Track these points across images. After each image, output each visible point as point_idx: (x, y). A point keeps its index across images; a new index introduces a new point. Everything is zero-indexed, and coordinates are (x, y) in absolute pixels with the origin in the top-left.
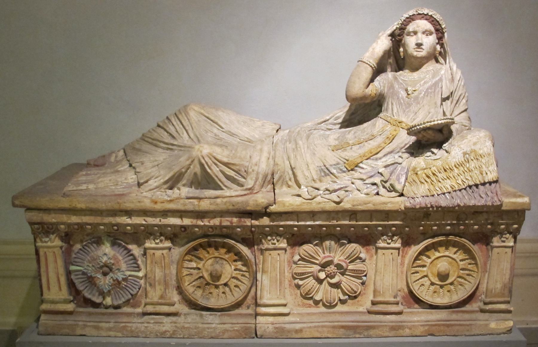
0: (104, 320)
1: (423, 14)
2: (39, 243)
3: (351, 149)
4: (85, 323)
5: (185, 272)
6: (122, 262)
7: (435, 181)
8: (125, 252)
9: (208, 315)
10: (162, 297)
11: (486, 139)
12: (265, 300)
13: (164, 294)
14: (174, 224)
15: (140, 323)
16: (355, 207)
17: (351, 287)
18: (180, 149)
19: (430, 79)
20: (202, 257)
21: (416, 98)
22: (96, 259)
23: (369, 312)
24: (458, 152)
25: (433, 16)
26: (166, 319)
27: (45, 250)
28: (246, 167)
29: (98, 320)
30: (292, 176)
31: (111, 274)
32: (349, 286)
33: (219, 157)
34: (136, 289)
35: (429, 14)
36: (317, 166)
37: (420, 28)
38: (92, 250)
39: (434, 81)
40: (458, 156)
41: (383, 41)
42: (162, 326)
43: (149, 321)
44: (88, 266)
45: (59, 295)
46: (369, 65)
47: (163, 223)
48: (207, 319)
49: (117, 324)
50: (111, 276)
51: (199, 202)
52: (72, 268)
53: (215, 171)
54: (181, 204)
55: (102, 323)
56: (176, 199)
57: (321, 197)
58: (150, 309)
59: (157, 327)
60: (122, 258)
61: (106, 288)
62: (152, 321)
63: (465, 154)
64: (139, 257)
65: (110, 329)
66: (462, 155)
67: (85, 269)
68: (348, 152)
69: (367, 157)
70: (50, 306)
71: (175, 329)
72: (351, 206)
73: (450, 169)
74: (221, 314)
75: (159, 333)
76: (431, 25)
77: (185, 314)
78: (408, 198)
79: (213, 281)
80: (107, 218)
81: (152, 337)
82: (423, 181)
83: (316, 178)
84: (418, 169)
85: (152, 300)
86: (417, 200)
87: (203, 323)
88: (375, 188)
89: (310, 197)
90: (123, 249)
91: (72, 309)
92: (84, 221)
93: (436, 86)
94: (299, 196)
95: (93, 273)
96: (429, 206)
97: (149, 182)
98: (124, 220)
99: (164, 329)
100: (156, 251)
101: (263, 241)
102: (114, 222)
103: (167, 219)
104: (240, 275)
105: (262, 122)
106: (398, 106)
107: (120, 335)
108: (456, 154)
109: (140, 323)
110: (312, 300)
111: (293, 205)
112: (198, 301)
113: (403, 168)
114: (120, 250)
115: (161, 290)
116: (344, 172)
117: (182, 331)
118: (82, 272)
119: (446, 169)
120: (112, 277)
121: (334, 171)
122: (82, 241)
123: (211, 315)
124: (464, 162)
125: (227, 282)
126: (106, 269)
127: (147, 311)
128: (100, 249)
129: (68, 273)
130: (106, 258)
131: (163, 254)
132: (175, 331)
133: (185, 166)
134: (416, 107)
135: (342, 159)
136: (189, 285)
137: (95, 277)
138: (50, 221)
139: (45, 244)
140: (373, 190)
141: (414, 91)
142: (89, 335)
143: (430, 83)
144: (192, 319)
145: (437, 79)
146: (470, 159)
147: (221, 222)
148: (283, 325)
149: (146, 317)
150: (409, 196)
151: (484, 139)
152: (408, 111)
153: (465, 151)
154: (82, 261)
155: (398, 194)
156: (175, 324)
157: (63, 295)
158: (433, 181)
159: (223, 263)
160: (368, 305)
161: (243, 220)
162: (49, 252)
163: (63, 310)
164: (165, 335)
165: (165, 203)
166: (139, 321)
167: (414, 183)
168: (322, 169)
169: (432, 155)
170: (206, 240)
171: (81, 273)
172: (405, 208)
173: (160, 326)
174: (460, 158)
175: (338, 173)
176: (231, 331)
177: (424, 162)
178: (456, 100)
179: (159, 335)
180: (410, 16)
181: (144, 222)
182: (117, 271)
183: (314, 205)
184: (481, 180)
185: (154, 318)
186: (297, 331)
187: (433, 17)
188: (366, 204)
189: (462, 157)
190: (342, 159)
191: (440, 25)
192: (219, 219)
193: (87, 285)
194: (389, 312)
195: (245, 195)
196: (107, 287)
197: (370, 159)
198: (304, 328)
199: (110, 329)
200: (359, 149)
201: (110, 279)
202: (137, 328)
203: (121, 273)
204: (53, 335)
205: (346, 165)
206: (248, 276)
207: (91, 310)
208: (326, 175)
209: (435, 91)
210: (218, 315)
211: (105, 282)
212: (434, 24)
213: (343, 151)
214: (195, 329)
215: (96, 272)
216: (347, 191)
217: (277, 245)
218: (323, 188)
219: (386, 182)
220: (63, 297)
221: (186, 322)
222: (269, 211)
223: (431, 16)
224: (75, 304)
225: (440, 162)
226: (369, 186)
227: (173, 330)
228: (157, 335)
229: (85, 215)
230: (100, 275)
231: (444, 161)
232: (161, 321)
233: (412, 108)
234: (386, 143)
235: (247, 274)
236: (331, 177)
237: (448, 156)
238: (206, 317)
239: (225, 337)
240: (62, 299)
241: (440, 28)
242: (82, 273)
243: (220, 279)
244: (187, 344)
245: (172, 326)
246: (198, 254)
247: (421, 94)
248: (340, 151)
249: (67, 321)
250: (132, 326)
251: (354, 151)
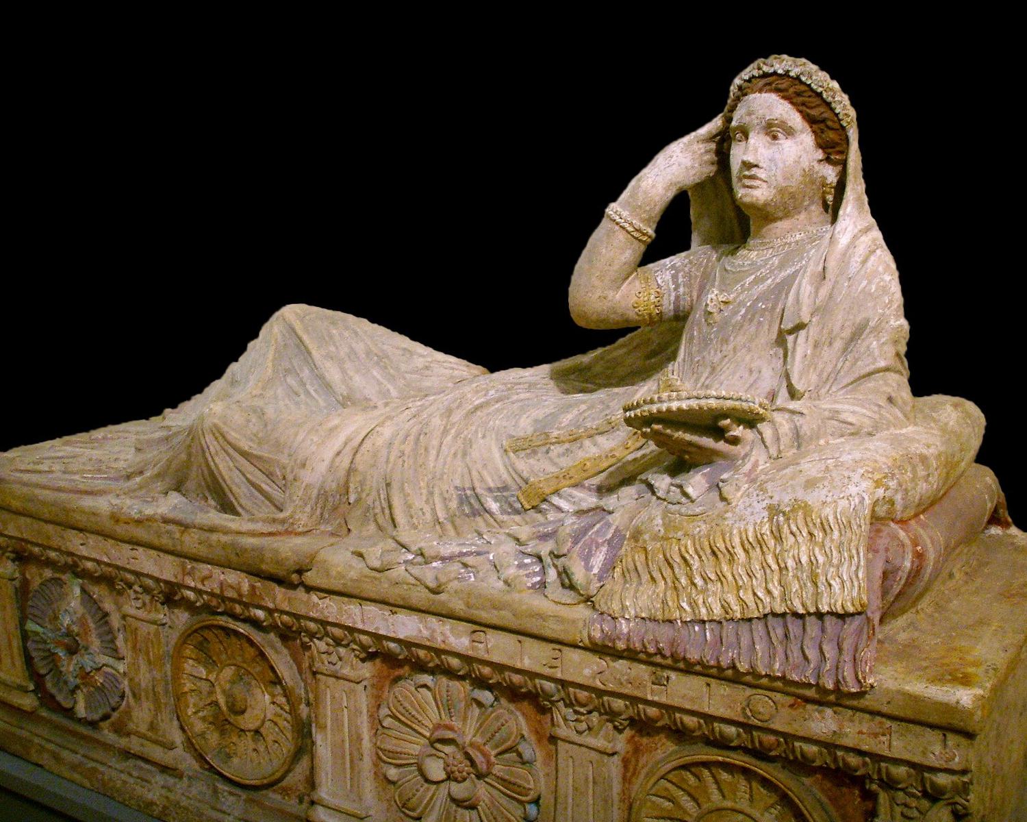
0: (70, 746)
1: (775, 73)
3: (547, 452)
4: (43, 743)
7: (684, 581)
10: (152, 727)
11: (851, 474)
13: (155, 721)
19: (771, 271)
21: (726, 322)
24: (755, 503)
25: (803, 79)
26: (160, 779)
28: (284, 468)
30: (385, 505)
33: (233, 435)
35: (792, 74)
36: (456, 487)
37: (753, 117)
39: (784, 274)
40: (752, 514)
41: (671, 157)
46: (617, 224)
49: (85, 760)
51: (183, 532)
53: (221, 466)
56: (147, 520)
57: (406, 570)
59: (139, 790)
62: (135, 774)
63: (774, 511)
64: (119, 630)
65: (74, 767)
66: (766, 514)
67: (44, 633)
68: (538, 460)
69: (572, 481)
71: (165, 803)
72: (463, 607)
73: (727, 548)
75: (143, 802)
76: (790, 106)
77: (190, 778)
78: (602, 614)
82: (656, 575)
83: (445, 519)
84: (646, 537)
86: (624, 627)
87: (213, 808)
88: (538, 569)
89: (377, 564)
91: (28, 708)
93: (780, 293)
94: (361, 555)
96: (652, 650)
99: (150, 796)
105: (430, 360)
107: (88, 785)
108: (749, 509)
111: (344, 577)
113: (608, 525)
115: (150, 710)
116: (517, 512)
119: (715, 549)
121: (494, 506)
123: (231, 793)
124: (765, 537)
125: (260, 728)
127: (130, 749)
129: (25, 636)
134: (718, 352)
136: (195, 713)
137: (54, 654)
140: (527, 576)
141: (725, 303)
143: (769, 281)
144: (200, 792)
145: (789, 271)
146: (785, 529)
149: (131, 762)
150: (605, 609)
151: (846, 474)
152: (698, 362)
153: (775, 501)
155: (582, 598)
156: (169, 794)
158: (677, 579)
159: (249, 684)
167: (633, 574)
168: (465, 494)
169: (684, 500)
174: (759, 522)
175: (503, 512)
177: (662, 519)
178: (842, 338)
180: (745, 81)
183: (386, 586)
184: (809, 603)
187: (804, 84)
188: (495, 608)
189: (766, 520)
191: (828, 104)
195: (270, 534)
197: (583, 486)
200: (563, 454)
203: (90, 657)
205: (519, 493)
207: (57, 718)
208: (475, 513)
209: (773, 308)
211: (69, 666)
212: (803, 104)
213: (528, 456)
216: (465, 566)
217: (338, 667)
218: (414, 548)
219: (558, 557)
221: (186, 794)
223: (798, 78)
224: (39, 698)
225: (703, 527)
226: (527, 561)
230: (64, 653)
231: (713, 524)
232: (149, 777)
233: (710, 353)
234: (627, 448)
236: (485, 521)
237: (726, 512)
238: (224, 797)
241: (828, 114)
245: (161, 795)
247: (736, 313)
248: (522, 454)
249: (22, 728)
251: (551, 459)
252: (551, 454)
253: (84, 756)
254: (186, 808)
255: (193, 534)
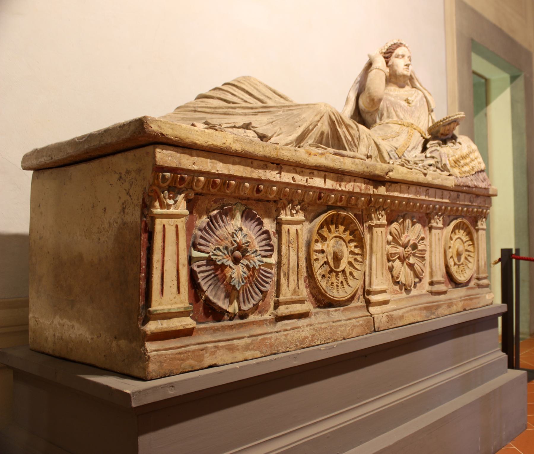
2: (158, 209)
5: (314, 256)
6: (256, 242)
8: (258, 227)
9: (333, 312)
10: (295, 292)
12: (375, 287)
14: (318, 186)
15: (277, 332)
16: (434, 180)
17: (421, 268)
18: (289, 108)
20: (326, 236)
22: (227, 238)
23: (432, 293)
27: (165, 221)
29: (229, 337)
31: (244, 261)
32: (420, 267)
34: (267, 283)
38: (219, 226)
42: (301, 330)
43: (284, 328)
44: (218, 249)
45: (176, 303)
47: (309, 185)
48: (333, 316)
50: (245, 264)
52: (195, 254)
54: (331, 159)
55: (235, 341)
58: (283, 310)
60: (255, 238)
61: (239, 282)
65: (247, 348)
70: (162, 324)
71: (314, 333)
74: (344, 308)
79: (335, 268)
80: (257, 171)
81: (292, 349)
85: (286, 298)
90: (256, 223)
92: (231, 173)
95: (226, 260)
97: (272, 139)
98: (272, 175)
99: (303, 334)
100: (291, 226)
101: (373, 215)
102: (263, 178)
103: (313, 179)
104: (354, 258)
106: (403, 113)
109: (277, 332)
110: (398, 286)
112: (327, 293)
114: (251, 226)
117: (320, 335)
118: (205, 261)
120: (247, 266)
122: (208, 212)
123: (336, 311)
126: (238, 253)
128: (229, 224)
130: (241, 236)
131: (297, 230)
132: (313, 335)
133: (313, 122)
135: (393, 147)
138: (189, 167)
139: (165, 211)
142: (220, 363)
147: (353, 189)
148: (392, 313)
154: (207, 243)
156: (313, 327)
157: (182, 302)
160: (427, 287)
161: (368, 188)
162: (170, 225)
163: (181, 328)
164: (304, 344)
165: (317, 156)
166: (276, 330)
170: (335, 212)
171: (204, 262)
172: (455, 185)
173: (299, 331)
176: (358, 326)
179: (299, 344)
181: (292, 182)
182: (253, 255)
185: (287, 324)
186: (402, 317)
190: (393, 147)
192: (352, 183)
193: (210, 283)
194: (440, 291)
196: (241, 281)
198: (404, 313)
199: (247, 348)
201: (243, 269)
202: (277, 339)
204: (169, 376)
206: (361, 260)
210: (341, 310)
214: (331, 329)
215: (228, 257)
220: (182, 305)
222: (389, 178)
227: (312, 334)
228: (297, 345)
229: (234, 163)
235: (359, 258)
239: (353, 335)
240: (182, 308)
242: (207, 263)
243: (340, 265)
244: (335, 346)
246: (323, 231)
250: (271, 337)
252: (394, 141)
253: (249, 337)
254: (325, 328)
255: (348, 160)
